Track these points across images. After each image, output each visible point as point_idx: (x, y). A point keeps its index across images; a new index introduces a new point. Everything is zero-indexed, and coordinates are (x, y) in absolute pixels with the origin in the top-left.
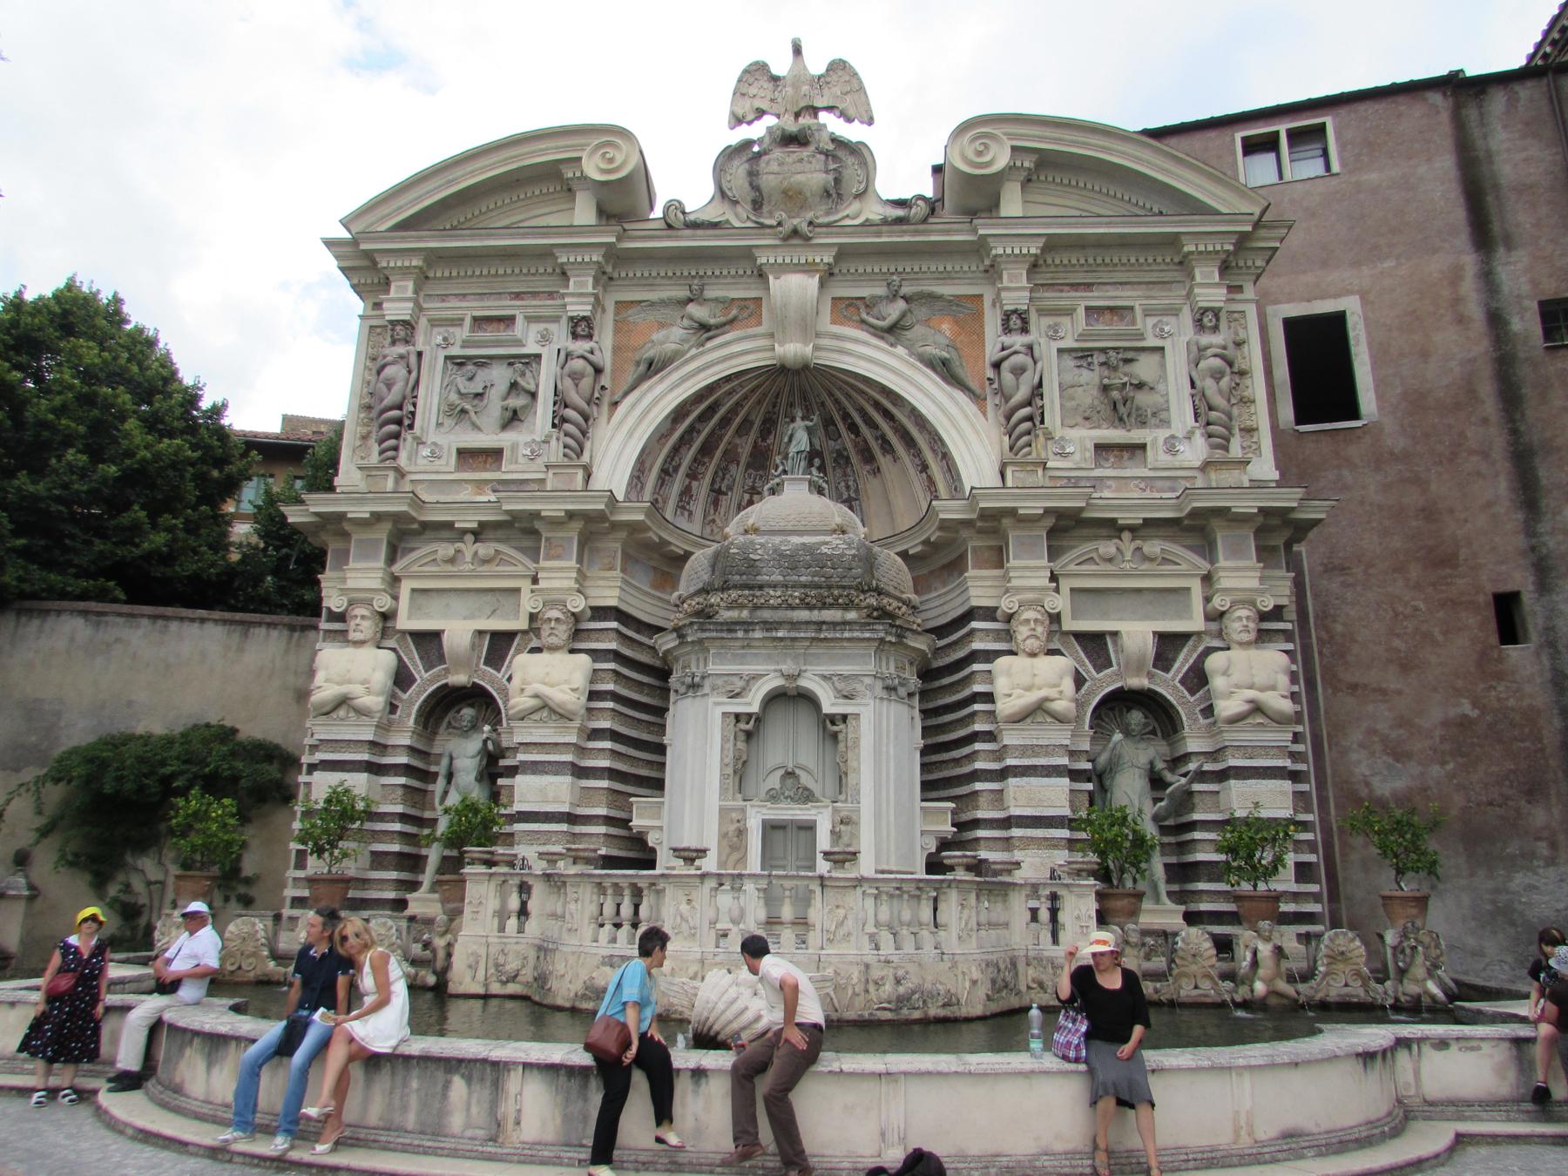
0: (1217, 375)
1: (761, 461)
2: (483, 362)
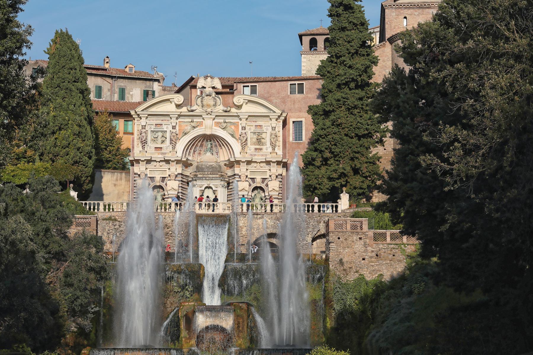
0: (274, 138)
1: (202, 146)
2: (157, 132)
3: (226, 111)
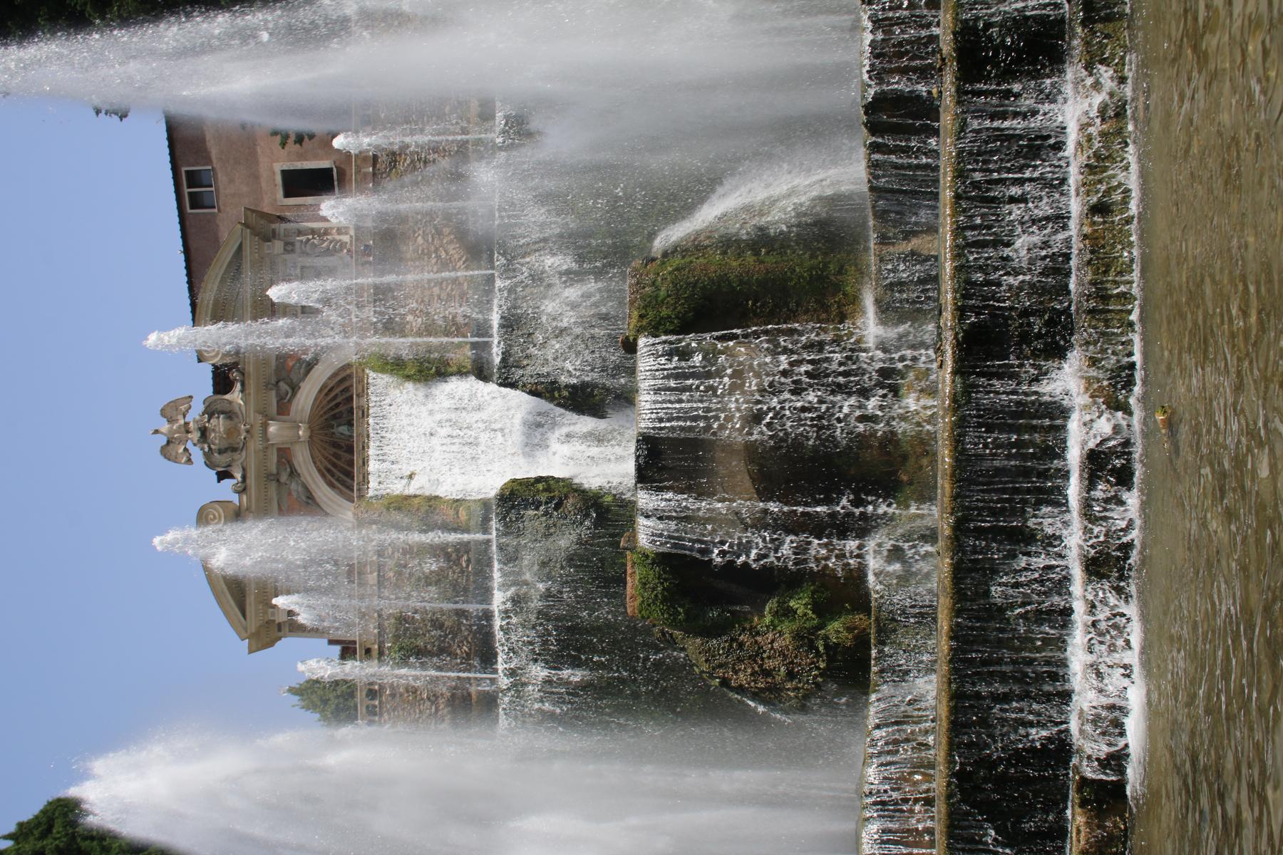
3: (243, 385)
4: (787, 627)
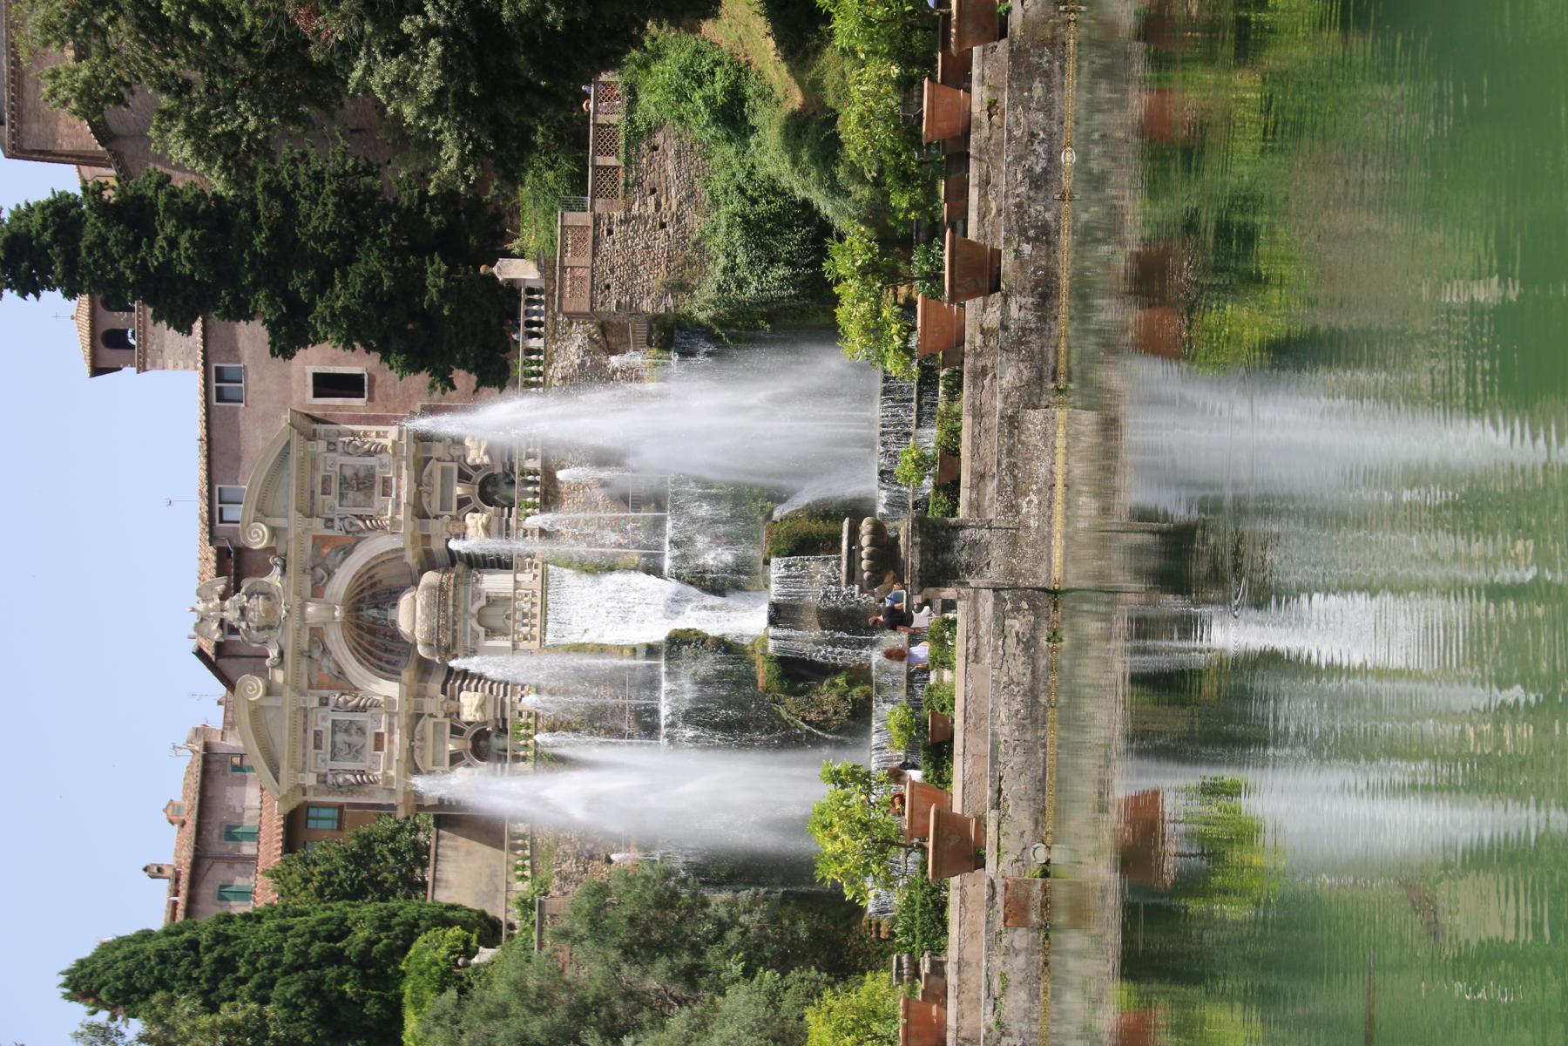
3: (284, 569)
4: (834, 691)
